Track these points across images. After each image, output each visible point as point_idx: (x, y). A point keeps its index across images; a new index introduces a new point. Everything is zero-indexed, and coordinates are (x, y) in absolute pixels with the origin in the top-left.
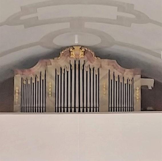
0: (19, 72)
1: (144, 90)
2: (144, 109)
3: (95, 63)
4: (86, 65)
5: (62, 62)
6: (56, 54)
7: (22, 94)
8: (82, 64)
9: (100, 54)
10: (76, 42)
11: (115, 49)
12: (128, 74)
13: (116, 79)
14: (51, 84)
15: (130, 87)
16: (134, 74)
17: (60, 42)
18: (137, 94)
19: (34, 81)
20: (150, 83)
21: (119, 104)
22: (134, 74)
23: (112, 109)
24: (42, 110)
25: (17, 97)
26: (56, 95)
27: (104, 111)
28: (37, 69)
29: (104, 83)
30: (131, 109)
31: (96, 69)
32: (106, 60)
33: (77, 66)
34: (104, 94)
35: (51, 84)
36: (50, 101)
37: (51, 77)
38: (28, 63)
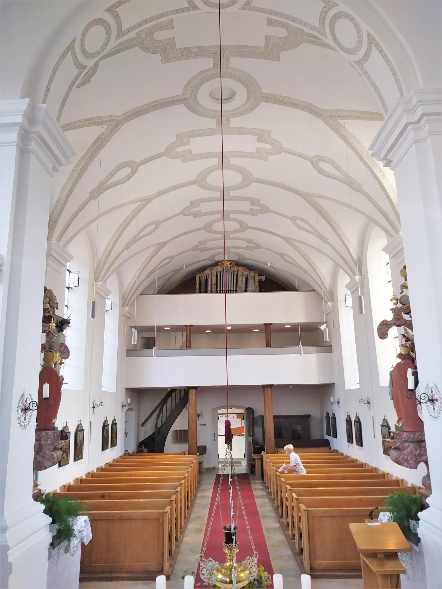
0: (198, 273)
1: (260, 281)
2: (260, 291)
3: (236, 269)
4: (232, 269)
5: (219, 268)
6: (216, 264)
7: (200, 284)
8: (229, 268)
9: (238, 264)
10: (226, 258)
11: (246, 261)
12: (252, 274)
13: (246, 276)
14: (214, 279)
15: (253, 280)
16: (255, 274)
17: (218, 258)
18: (257, 284)
19: (205, 278)
20: (263, 278)
21: (247, 288)
22: (255, 274)
23: (244, 291)
24: (210, 292)
25: (197, 286)
26: (216, 284)
27: (240, 292)
28: (207, 272)
29: (240, 278)
30: (254, 291)
31: (236, 272)
32: (241, 267)
33: (227, 270)
34: (240, 284)
35: (214, 279)
36: (214, 287)
37: (214, 275)
38: (203, 269)
